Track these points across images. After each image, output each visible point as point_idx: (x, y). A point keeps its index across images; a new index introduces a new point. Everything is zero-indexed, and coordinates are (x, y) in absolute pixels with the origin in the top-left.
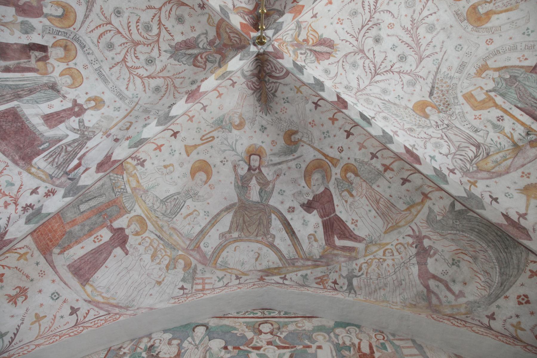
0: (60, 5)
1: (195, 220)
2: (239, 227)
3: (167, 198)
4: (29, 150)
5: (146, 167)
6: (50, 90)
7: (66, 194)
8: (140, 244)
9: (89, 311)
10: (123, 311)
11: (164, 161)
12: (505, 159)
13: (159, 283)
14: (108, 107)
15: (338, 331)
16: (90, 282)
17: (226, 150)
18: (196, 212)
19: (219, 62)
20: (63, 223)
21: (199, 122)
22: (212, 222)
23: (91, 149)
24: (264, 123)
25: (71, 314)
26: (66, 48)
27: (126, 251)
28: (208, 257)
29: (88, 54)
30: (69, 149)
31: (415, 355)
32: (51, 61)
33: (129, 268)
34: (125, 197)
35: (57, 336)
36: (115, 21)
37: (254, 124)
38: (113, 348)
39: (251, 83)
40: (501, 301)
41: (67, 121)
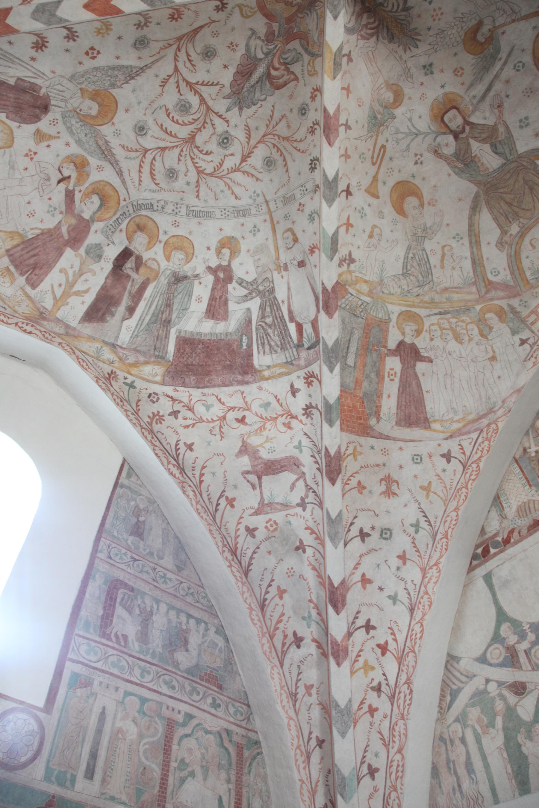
0: (89, 193)
1: (455, 257)
2: (510, 216)
3: (405, 265)
4: (239, 360)
5: (357, 259)
6: (179, 284)
7: (330, 367)
8: (432, 340)
9: (460, 445)
10: (492, 417)
11: (364, 232)
14: (243, 238)
16: (431, 420)
17: (409, 145)
18: (446, 249)
19: (306, 50)
20: (351, 393)
21: (356, 148)
22: (474, 241)
23: (289, 298)
24: (423, 60)
25: (449, 461)
26: (140, 228)
27: (427, 359)
28: (512, 283)
29: (163, 208)
30: (269, 320)
32: (146, 256)
33: (449, 372)
34: (371, 309)
35: (461, 489)
36: (148, 142)
37: (412, 77)
38: (517, 457)
39: (364, 30)
41: (228, 296)
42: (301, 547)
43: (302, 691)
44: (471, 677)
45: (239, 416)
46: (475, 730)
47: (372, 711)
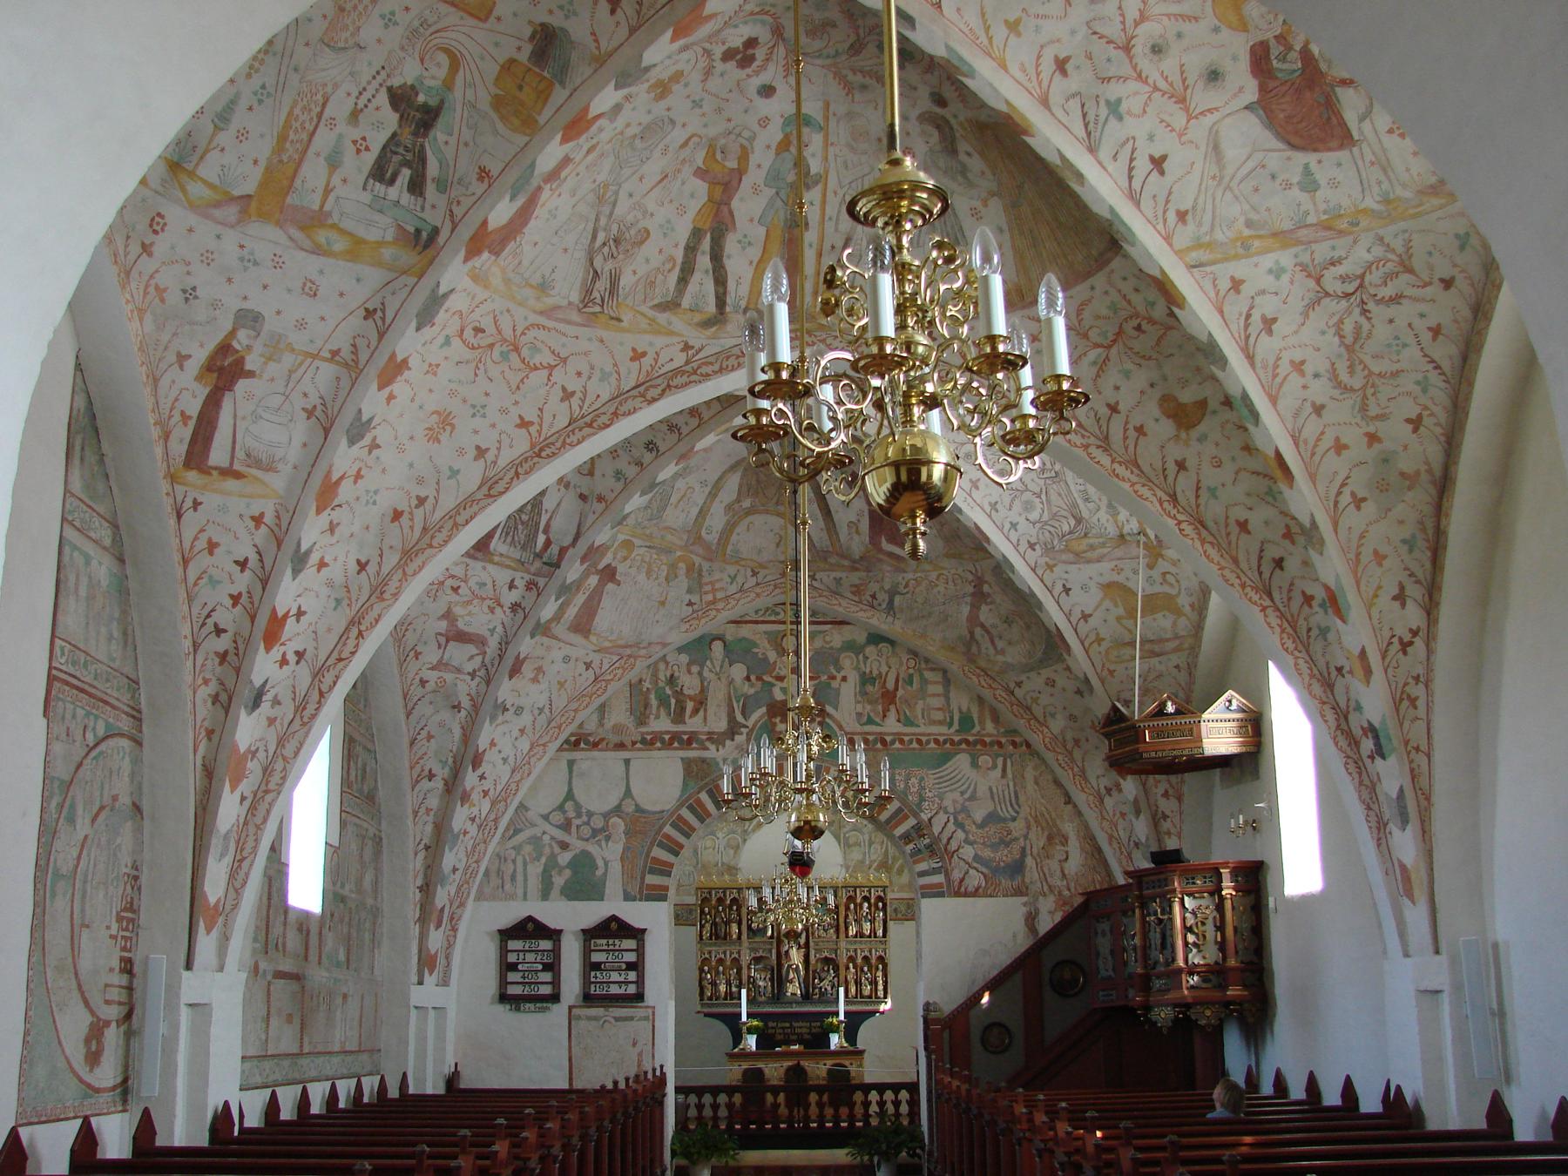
12: (1103, 545)
13: (663, 603)
15: (870, 650)
31: (938, 695)
40: (1033, 675)
42: (457, 707)
43: (423, 810)
44: (533, 825)
45: (455, 583)
46: (525, 859)
47: (465, 833)
